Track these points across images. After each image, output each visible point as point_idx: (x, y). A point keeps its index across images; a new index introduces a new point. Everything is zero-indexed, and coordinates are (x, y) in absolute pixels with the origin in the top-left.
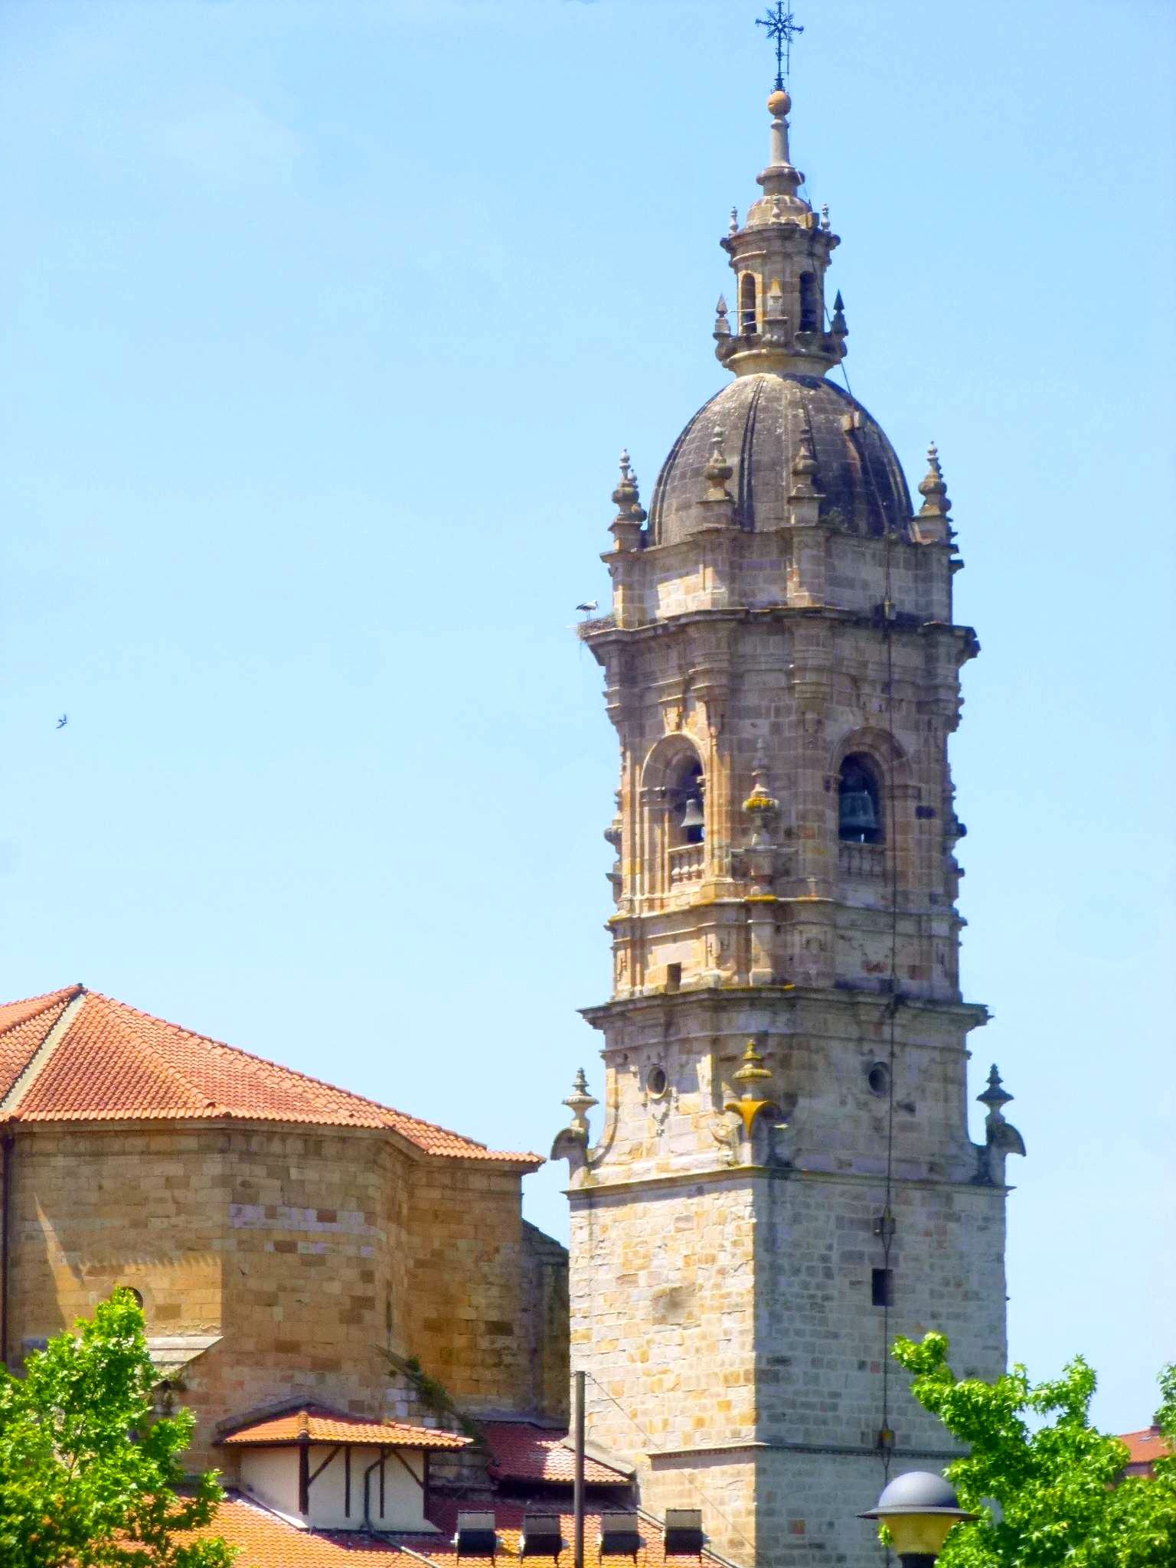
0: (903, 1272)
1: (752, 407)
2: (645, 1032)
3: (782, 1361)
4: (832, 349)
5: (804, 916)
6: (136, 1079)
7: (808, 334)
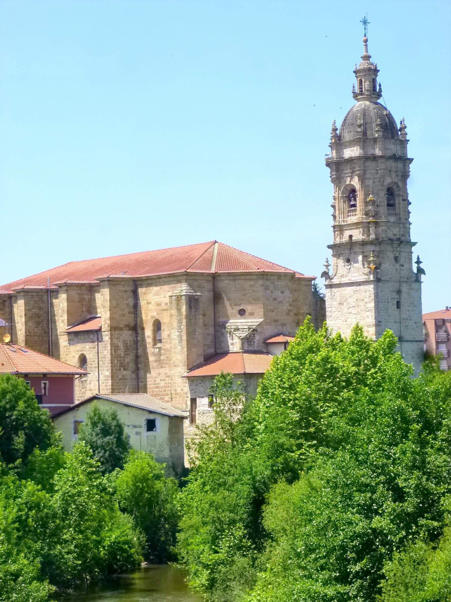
0: (402, 301)
1: (364, 109)
2: (344, 250)
3: (380, 322)
4: (379, 95)
5: (382, 224)
6: (238, 263)
7: (375, 93)
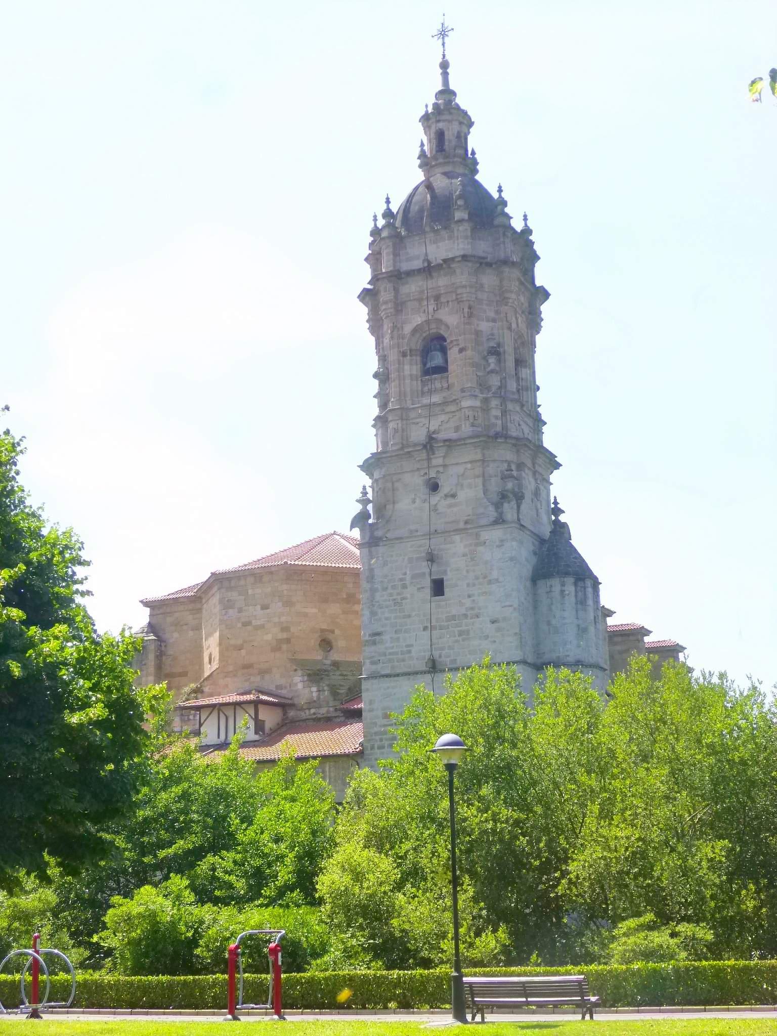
3: (378, 634)
